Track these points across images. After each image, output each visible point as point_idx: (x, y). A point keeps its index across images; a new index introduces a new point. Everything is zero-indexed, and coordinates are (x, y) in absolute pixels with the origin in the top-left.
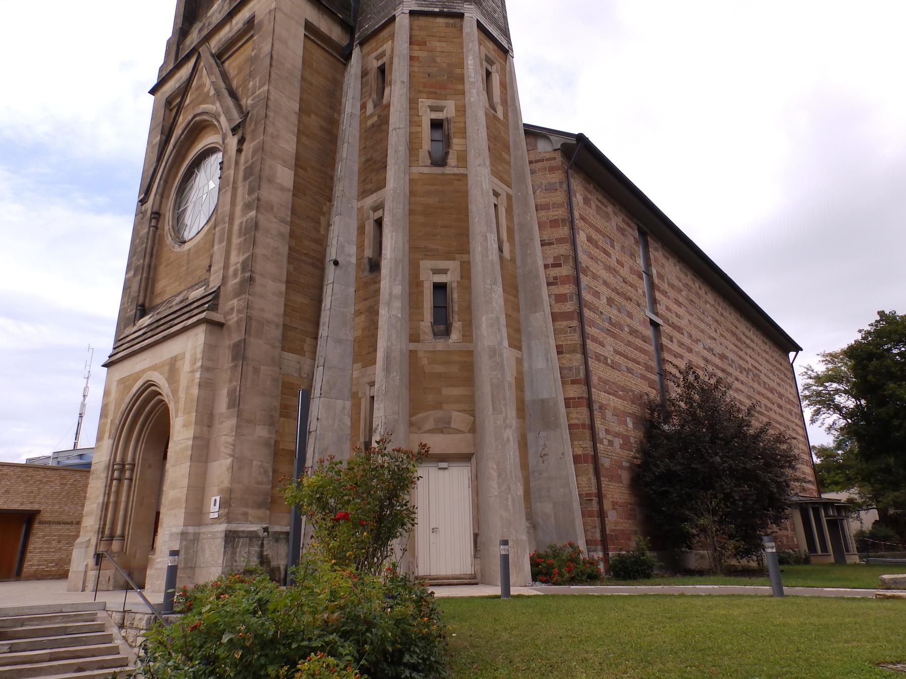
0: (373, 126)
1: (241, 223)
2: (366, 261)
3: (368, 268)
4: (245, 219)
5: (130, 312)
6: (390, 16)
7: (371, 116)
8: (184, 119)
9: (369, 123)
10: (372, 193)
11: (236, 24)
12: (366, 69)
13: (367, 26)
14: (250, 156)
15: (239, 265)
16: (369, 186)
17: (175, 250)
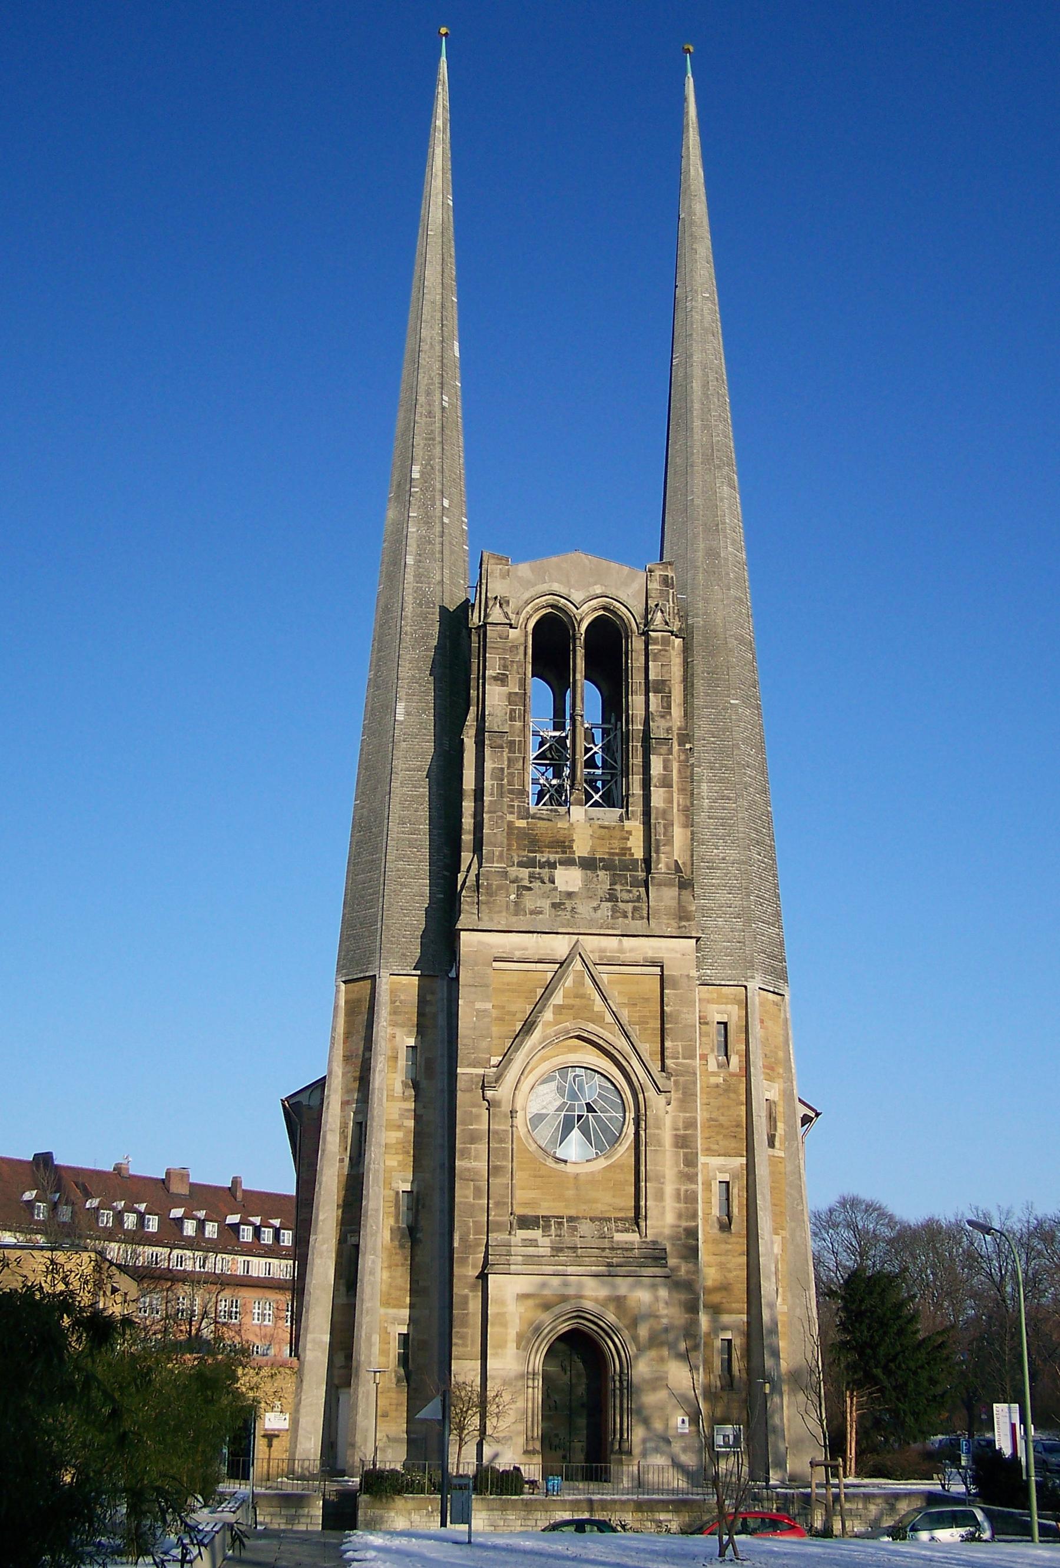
0: (717, 1086)
1: (678, 1190)
2: (715, 1218)
3: (717, 1226)
4: (683, 1188)
5: (495, 1216)
6: (740, 983)
7: (714, 1074)
8: (557, 1023)
9: (713, 1080)
10: (719, 1156)
11: (631, 950)
12: (705, 1018)
13: (708, 971)
14: (681, 1125)
15: (681, 1230)
16: (715, 1147)
17: (547, 1164)
